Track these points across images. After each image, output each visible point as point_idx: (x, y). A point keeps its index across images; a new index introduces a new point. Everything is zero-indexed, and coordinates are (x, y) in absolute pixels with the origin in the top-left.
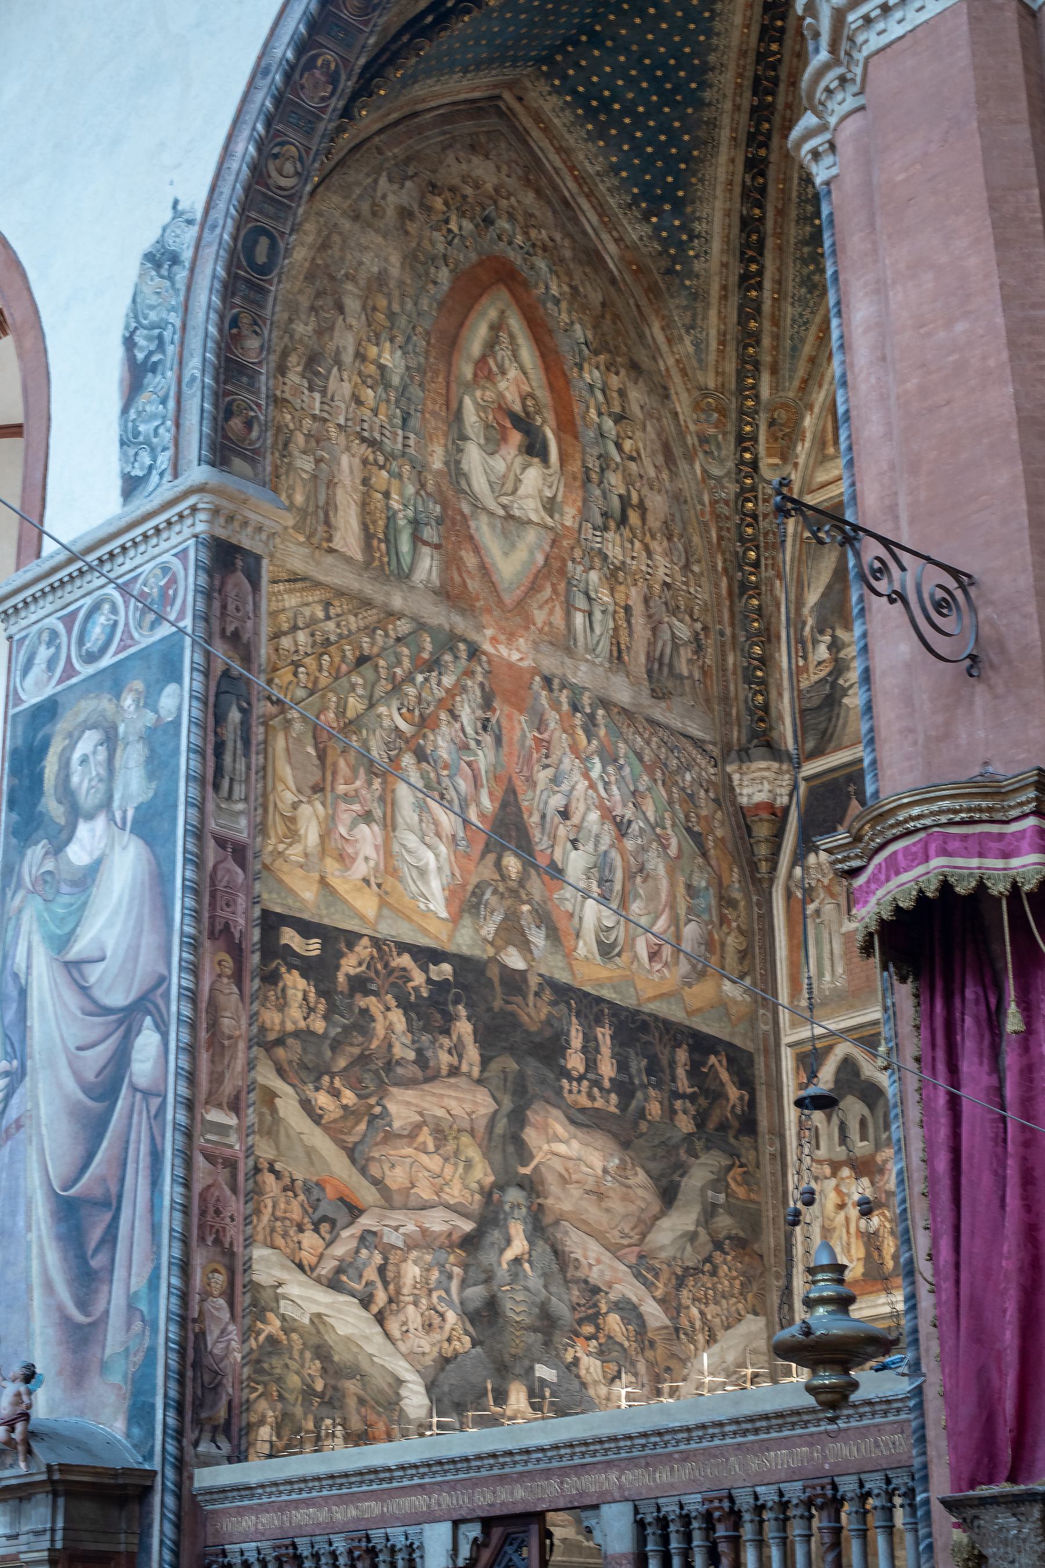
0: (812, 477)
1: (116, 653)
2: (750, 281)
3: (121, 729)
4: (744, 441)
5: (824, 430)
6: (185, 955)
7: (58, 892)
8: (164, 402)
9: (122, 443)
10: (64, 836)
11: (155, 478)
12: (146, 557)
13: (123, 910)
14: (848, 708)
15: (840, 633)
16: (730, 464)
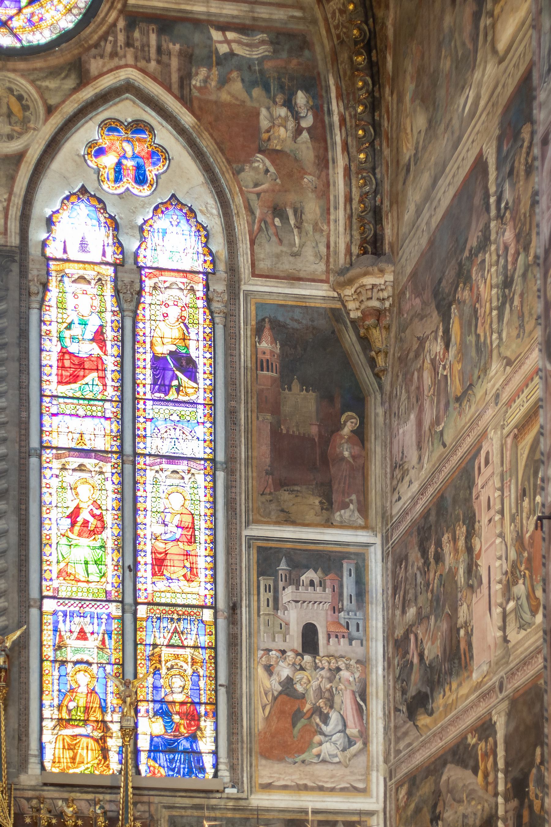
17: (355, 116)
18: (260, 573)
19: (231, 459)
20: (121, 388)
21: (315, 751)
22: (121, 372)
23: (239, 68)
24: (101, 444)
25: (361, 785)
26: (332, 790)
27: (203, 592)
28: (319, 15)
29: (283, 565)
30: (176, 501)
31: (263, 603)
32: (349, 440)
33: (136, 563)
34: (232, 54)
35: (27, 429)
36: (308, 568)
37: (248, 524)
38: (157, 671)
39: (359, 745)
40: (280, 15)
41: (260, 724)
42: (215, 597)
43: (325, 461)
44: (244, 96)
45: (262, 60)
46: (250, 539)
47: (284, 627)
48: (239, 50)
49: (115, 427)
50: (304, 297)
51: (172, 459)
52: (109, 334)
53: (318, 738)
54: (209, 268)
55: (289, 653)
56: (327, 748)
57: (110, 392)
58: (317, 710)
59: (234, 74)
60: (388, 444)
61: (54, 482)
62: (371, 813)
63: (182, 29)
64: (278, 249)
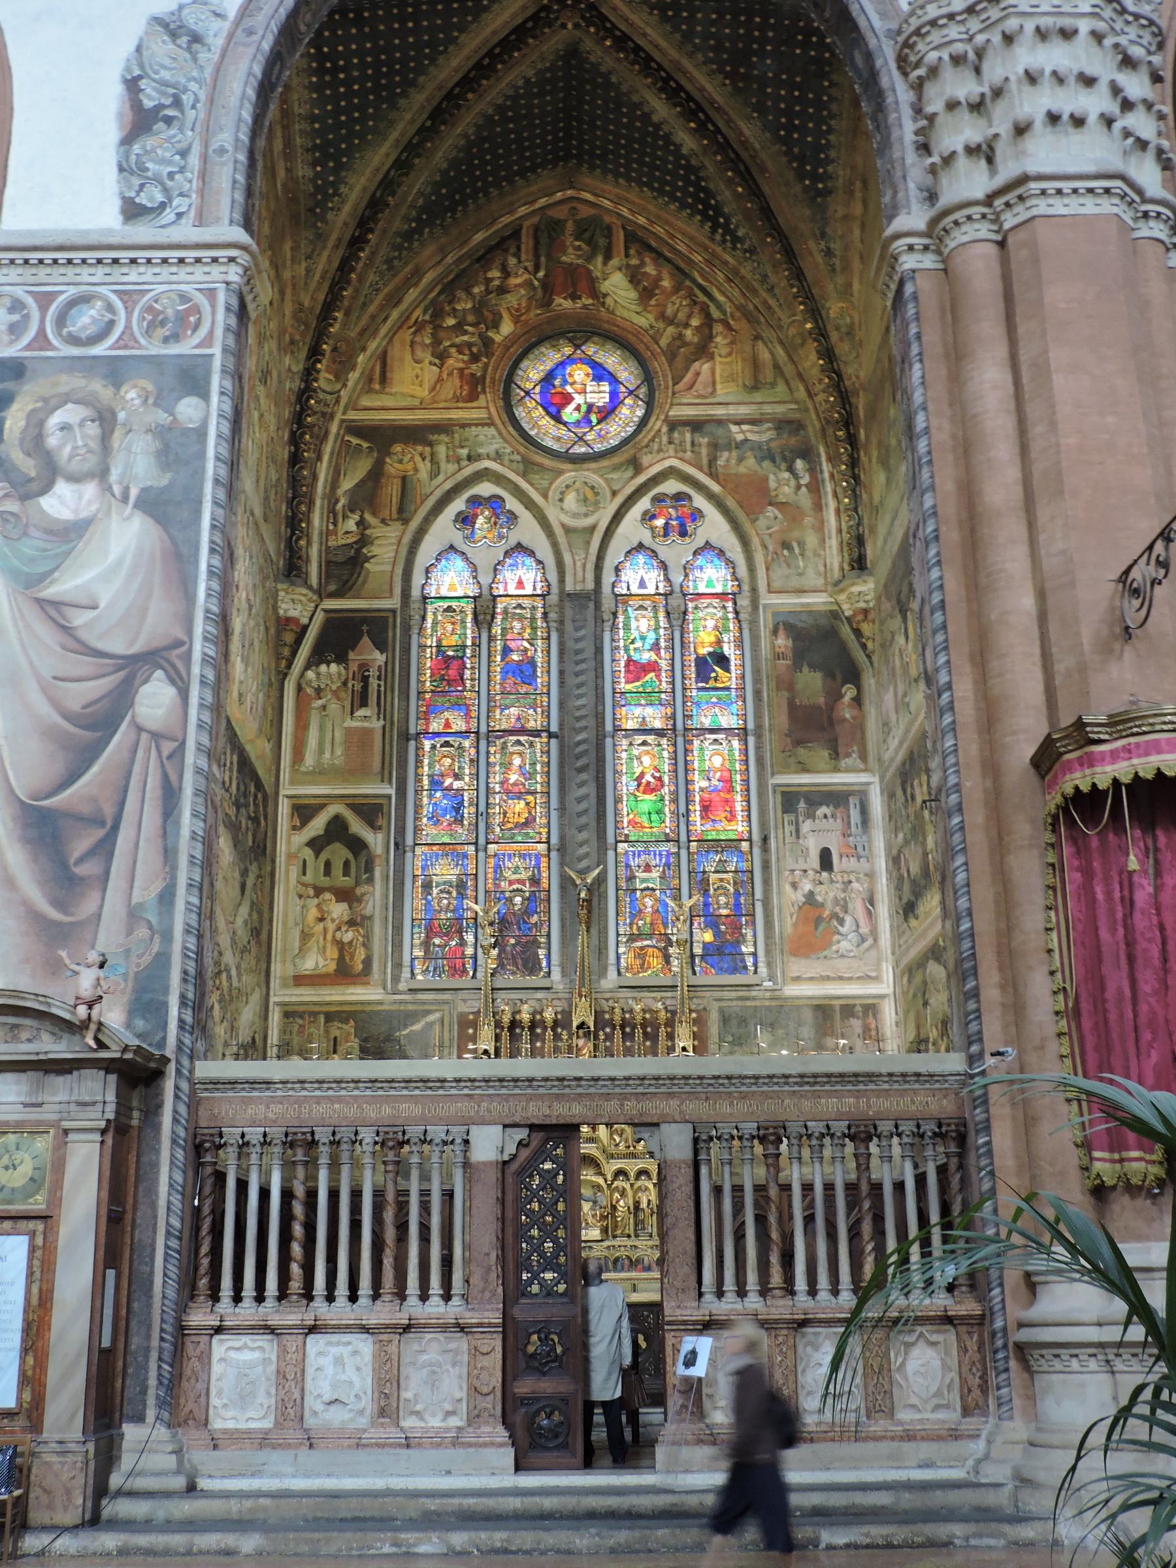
0: (358, 398)
1: (111, 348)
2: (357, 242)
3: (121, 416)
4: (315, 353)
5: (372, 370)
6: (209, 628)
7: (25, 534)
8: (184, 153)
9: (121, 169)
10: (34, 486)
11: (168, 216)
12: (158, 279)
13: (124, 571)
14: (368, 572)
15: (368, 516)
16: (301, 367)
17: (840, 472)
18: (784, 812)
19: (759, 726)
20: (673, 683)
21: (834, 948)
22: (673, 671)
23: (752, 449)
24: (658, 724)
25: (873, 974)
26: (850, 979)
27: (740, 829)
28: (811, 406)
29: (802, 805)
30: (717, 761)
31: (787, 834)
32: (850, 706)
33: (688, 810)
34: (746, 440)
35: (603, 718)
36: (821, 804)
37: (773, 774)
38: (707, 891)
39: (870, 941)
40: (780, 409)
41: (789, 929)
42: (750, 832)
43: (831, 722)
44: (757, 468)
45: (768, 442)
46: (775, 786)
47: (805, 852)
48: (750, 436)
49: (669, 711)
50: (808, 604)
51: (712, 731)
52: (663, 644)
53: (836, 937)
54: (736, 589)
55: (810, 872)
56: (845, 945)
57: (664, 686)
58: (834, 916)
59: (749, 454)
60: (879, 707)
61: (624, 755)
62: (883, 997)
63: (708, 428)
64: (786, 571)
